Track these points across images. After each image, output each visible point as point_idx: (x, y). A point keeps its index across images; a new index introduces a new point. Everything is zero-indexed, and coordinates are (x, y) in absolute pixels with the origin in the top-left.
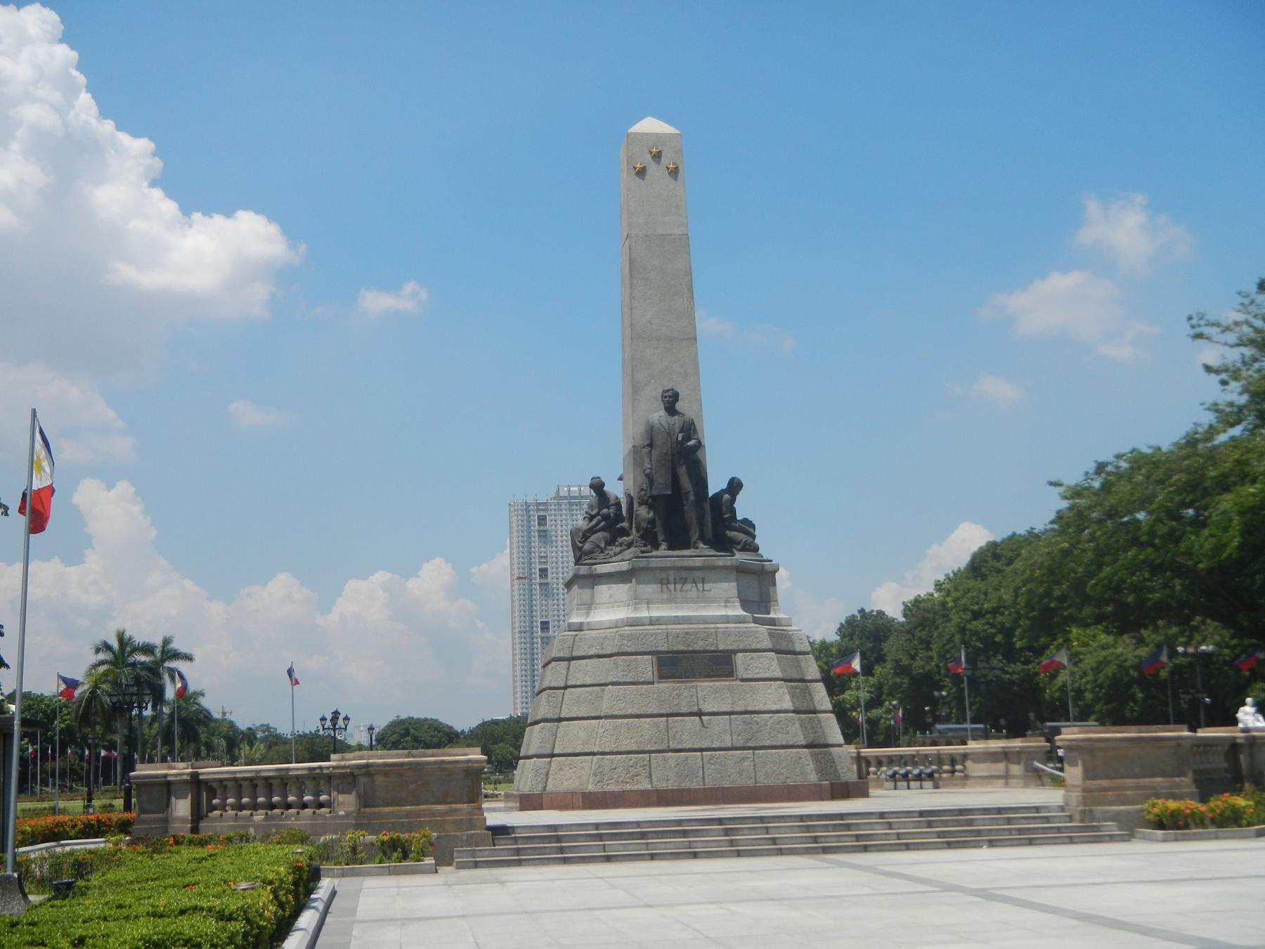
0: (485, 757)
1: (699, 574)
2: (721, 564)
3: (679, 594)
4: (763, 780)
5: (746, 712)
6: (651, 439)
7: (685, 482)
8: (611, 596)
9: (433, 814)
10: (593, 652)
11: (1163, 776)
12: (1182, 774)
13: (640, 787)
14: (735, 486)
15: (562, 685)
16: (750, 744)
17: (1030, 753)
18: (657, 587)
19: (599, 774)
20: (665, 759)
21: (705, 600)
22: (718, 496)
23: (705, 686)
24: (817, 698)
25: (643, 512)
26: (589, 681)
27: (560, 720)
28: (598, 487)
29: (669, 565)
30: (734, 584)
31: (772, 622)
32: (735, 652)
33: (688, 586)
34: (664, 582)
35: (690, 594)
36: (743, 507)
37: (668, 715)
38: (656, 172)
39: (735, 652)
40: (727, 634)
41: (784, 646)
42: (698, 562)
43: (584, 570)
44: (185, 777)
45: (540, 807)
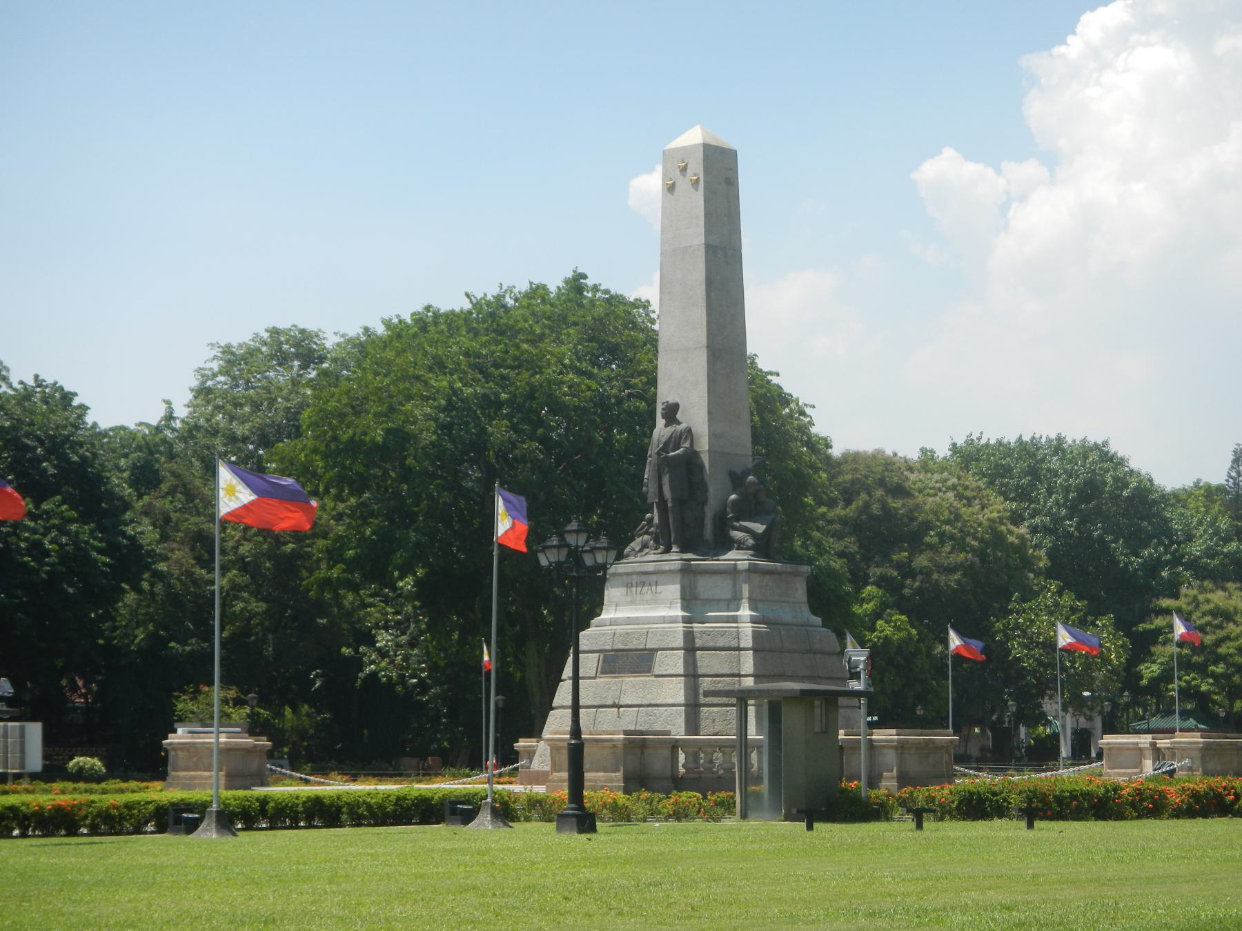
0: (264, 742)
1: (653, 578)
2: (667, 568)
3: (639, 597)
9: (202, 778)
11: (605, 772)
12: (617, 770)
17: (1184, 749)
18: (623, 590)
21: (656, 602)
23: (630, 680)
29: (630, 570)
30: (678, 587)
31: (735, 620)
32: (656, 650)
33: (646, 589)
34: (629, 585)
35: (648, 597)
38: (683, 185)
39: (656, 650)
42: (650, 567)
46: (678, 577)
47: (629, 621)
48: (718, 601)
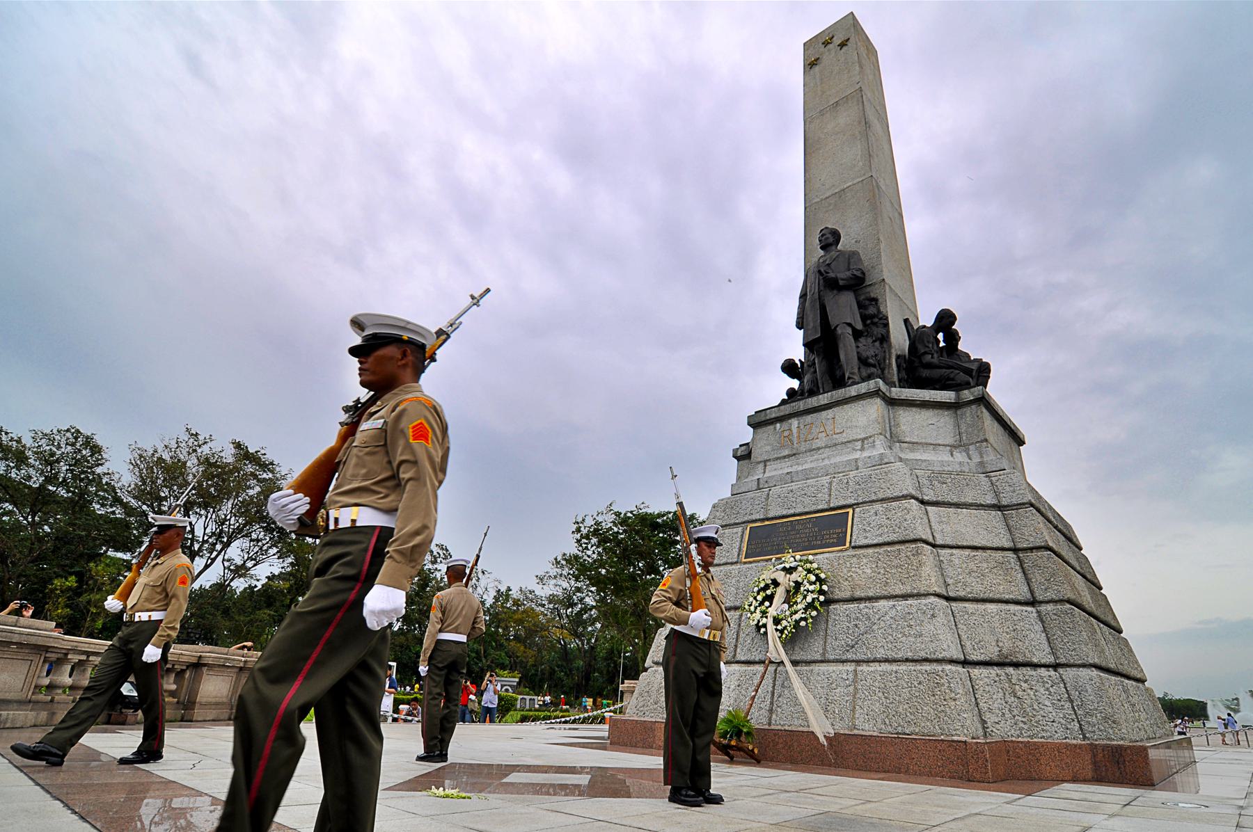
16: (849, 656)
28: (790, 368)
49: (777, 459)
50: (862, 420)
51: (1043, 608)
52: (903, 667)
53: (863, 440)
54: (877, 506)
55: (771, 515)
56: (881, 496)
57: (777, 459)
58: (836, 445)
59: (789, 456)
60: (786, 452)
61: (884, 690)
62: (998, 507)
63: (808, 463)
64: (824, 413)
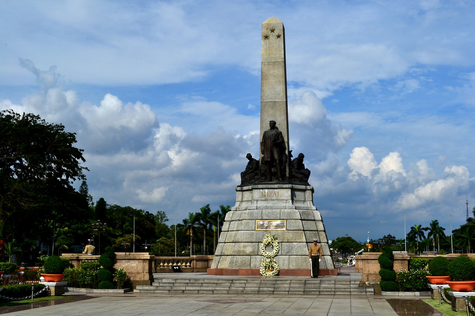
4: (291, 267)
5: (288, 242)
6: (265, 140)
7: (276, 156)
8: (247, 198)
10: (238, 218)
13: (246, 268)
14: (301, 156)
15: (227, 230)
19: (231, 263)
20: (256, 258)
22: (294, 160)
24: (321, 237)
25: (263, 168)
26: (235, 229)
27: (225, 243)
28: (249, 157)
36: (307, 164)
37: (259, 242)
38: (273, 37)
40: (284, 213)
41: (310, 218)
43: (239, 188)
44: (75, 258)
45: (222, 274)
46: (290, 190)
47: (267, 208)
48: (301, 201)
49: (261, 200)
50: (286, 195)
51: (322, 244)
52: (299, 256)
53: (286, 200)
54: (293, 221)
55: (264, 218)
56: (293, 218)
57: (261, 200)
58: (279, 200)
59: (264, 200)
60: (264, 199)
61: (296, 261)
62: (314, 220)
63: (270, 204)
64: (275, 190)
